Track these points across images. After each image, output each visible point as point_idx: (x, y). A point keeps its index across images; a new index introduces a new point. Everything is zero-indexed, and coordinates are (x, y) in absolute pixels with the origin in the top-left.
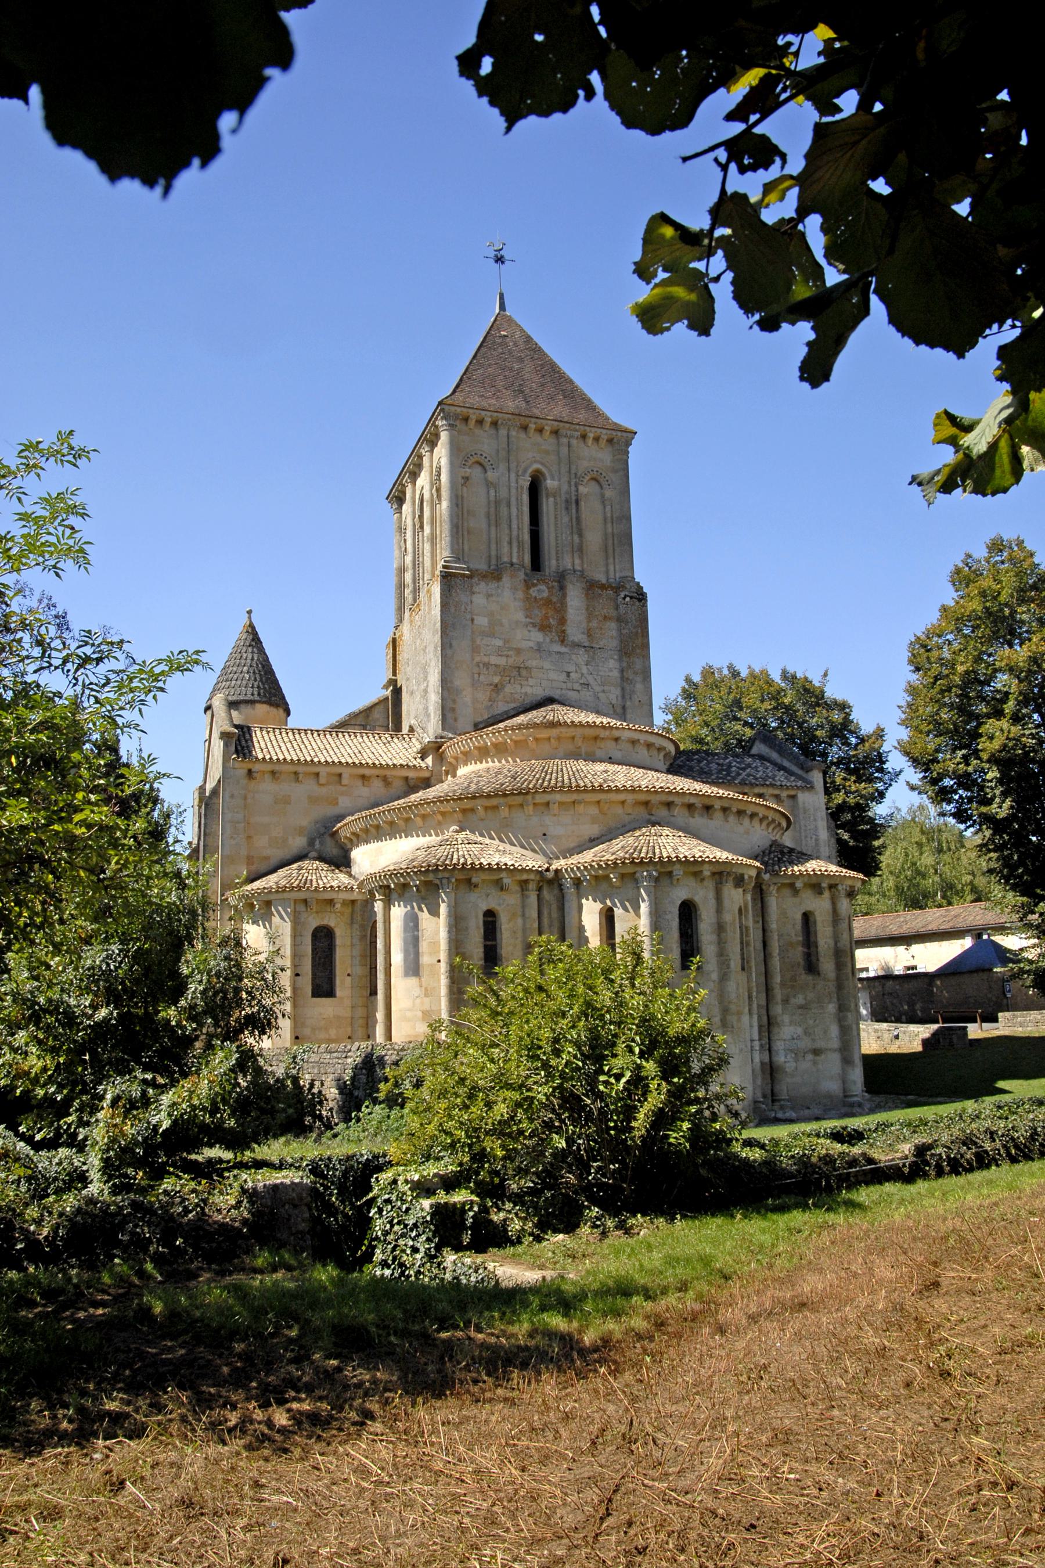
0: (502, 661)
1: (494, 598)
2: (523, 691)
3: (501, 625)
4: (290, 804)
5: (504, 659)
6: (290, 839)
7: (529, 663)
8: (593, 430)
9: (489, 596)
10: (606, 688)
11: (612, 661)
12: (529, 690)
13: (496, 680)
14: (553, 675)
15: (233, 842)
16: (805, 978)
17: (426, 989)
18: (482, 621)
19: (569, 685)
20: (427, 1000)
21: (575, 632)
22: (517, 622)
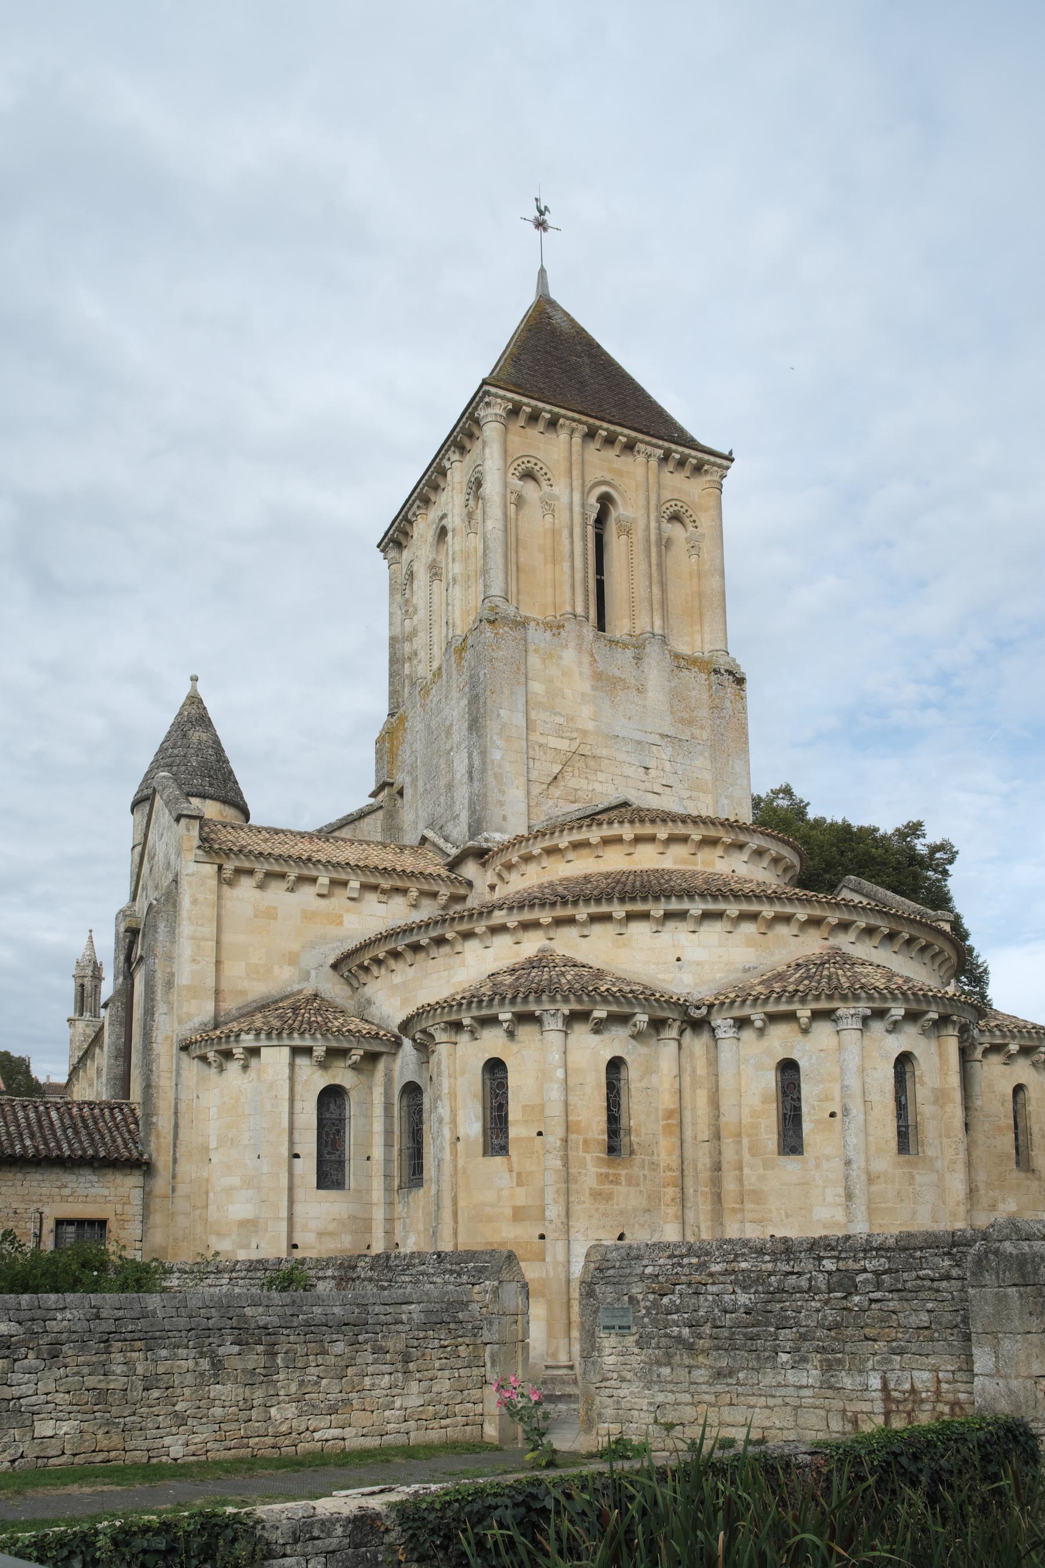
0: (563, 745)
2: (590, 788)
4: (275, 919)
5: (566, 742)
6: (276, 967)
7: (598, 752)
10: (694, 794)
12: (598, 787)
13: (556, 769)
14: (629, 771)
15: (196, 967)
16: (1015, 1176)
17: (519, 1175)
18: (537, 687)
19: (648, 786)
20: (521, 1191)
22: (583, 695)
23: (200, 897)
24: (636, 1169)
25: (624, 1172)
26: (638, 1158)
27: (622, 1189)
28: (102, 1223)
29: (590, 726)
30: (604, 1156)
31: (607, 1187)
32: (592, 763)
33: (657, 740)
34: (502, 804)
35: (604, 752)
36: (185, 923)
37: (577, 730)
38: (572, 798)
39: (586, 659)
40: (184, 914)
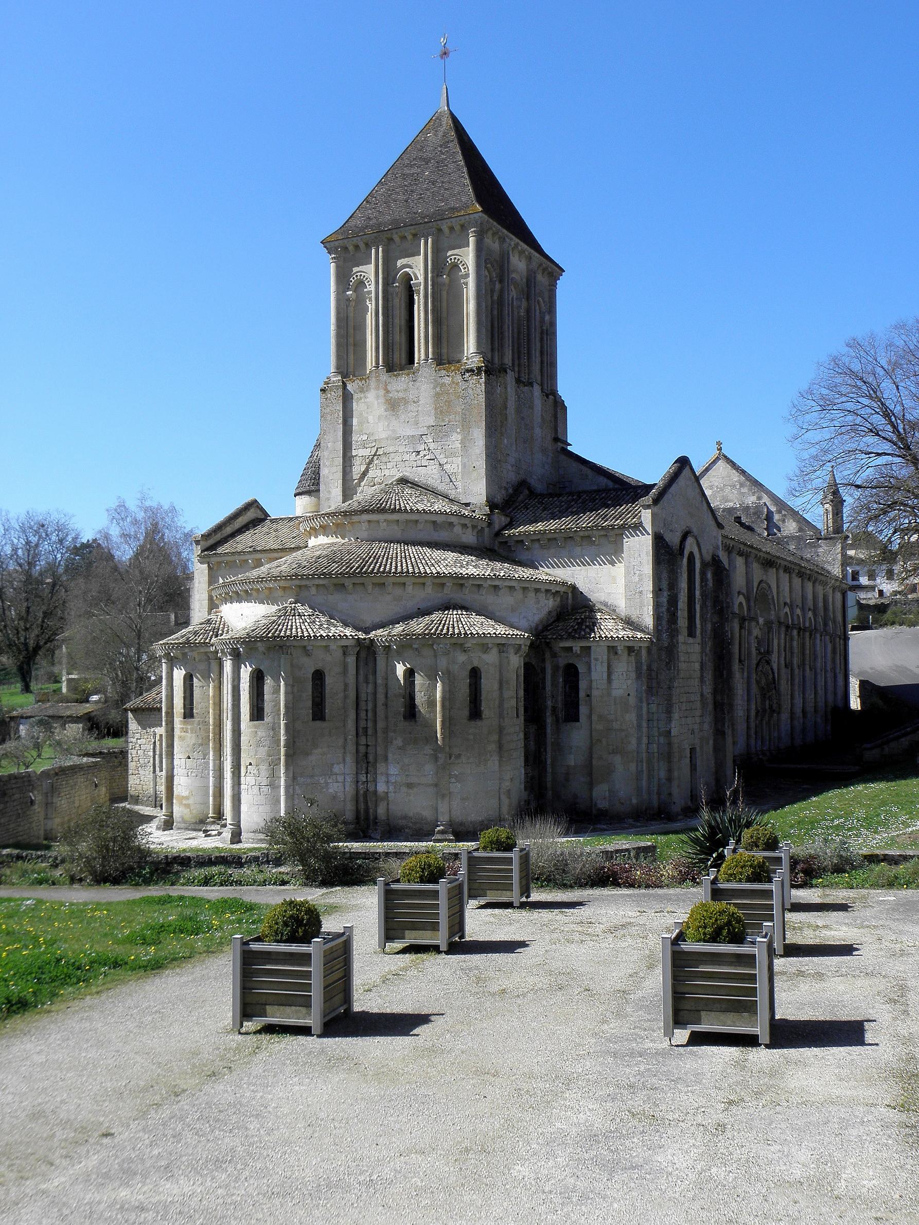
0: (367, 452)
1: (363, 401)
2: (383, 474)
10: (449, 460)
12: (387, 472)
13: (363, 468)
14: (406, 457)
19: (419, 463)
29: (383, 435)
32: (384, 459)
33: (424, 430)
34: (328, 499)
35: (391, 449)
36: (196, 593)
39: (382, 392)
40: (196, 589)
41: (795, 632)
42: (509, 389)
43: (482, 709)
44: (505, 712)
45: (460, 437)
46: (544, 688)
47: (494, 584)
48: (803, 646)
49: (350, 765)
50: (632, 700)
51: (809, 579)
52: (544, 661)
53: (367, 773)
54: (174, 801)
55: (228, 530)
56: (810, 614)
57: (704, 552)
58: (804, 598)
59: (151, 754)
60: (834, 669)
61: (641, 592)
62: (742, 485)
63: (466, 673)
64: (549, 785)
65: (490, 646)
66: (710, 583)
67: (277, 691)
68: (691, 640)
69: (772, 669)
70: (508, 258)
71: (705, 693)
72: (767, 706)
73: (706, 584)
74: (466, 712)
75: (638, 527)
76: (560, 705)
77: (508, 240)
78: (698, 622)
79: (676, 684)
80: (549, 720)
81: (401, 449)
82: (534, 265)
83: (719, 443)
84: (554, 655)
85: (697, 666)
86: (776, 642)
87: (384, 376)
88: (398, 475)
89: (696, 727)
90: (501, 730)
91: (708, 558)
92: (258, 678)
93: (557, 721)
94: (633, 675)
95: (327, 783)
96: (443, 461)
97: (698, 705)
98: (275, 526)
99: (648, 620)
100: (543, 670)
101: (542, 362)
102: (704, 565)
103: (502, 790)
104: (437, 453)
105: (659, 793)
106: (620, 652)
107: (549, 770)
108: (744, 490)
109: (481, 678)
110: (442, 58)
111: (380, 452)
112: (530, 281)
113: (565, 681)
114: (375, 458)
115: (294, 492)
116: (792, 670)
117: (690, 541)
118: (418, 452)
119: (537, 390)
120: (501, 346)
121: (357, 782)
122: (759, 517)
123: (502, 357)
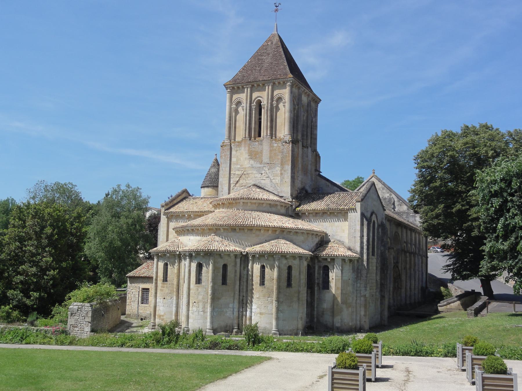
0: (240, 173)
1: (238, 151)
3: (240, 160)
8: (276, 80)
9: (236, 151)
10: (275, 178)
11: (278, 167)
12: (248, 182)
14: (257, 175)
19: (262, 178)
21: (266, 158)
22: (246, 158)
23: (164, 222)
24: (168, 285)
25: (165, 286)
26: (168, 283)
27: (165, 289)
28: (148, 289)
29: (248, 166)
30: (162, 282)
31: (162, 288)
32: (247, 176)
35: (250, 172)
36: (161, 228)
37: (243, 168)
38: (241, 186)
39: (247, 148)
40: (161, 226)
41: (408, 254)
42: (300, 149)
43: (292, 283)
44: (301, 284)
45: (280, 169)
46: (314, 275)
47: (296, 231)
48: (410, 260)
49: (236, 305)
50: (350, 282)
51: (414, 231)
52: (314, 264)
53: (243, 308)
54: (156, 317)
55: (175, 202)
56: (413, 247)
57: (379, 221)
58: (411, 239)
59: (137, 296)
60: (422, 270)
61: (355, 237)
62: (383, 189)
63: (286, 268)
64: (315, 316)
65: (296, 257)
66: (380, 234)
67: (208, 272)
68: (373, 257)
69: (399, 270)
70: (301, 96)
71: (377, 279)
72: (396, 286)
73: (379, 234)
74: (286, 284)
75: (354, 210)
76: (321, 282)
77: (301, 89)
78: (376, 249)
79: (368, 276)
80: (316, 289)
81: (254, 172)
82: (310, 99)
83: (374, 170)
84: (319, 261)
85: (375, 268)
86: (400, 258)
87: (248, 142)
88: (253, 183)
89: (374, 294)
90: (299, 292)
91: (380, 223)
92: (200, 267)
93: (319, 288)
94: (351, 271)
95: (226, 312)
96: (272, 178)
97: (375, 284)
98: (195, 201)
99: (358, 249)
100: (314, 268)
101: (311, 138)
102: (379, 226)
103: (299, 317)
104: (270, 175)
105: (360, 321)
106: (346, 261)
107: (316, 309)
108: (384, 191)
109: (292, 270)
110: (275, 12)
111: (245, 173)
112: (309, 104)
113: (323, 273)
114: (243, 175)
115: (201, 186)
116: (406, 271)
117: (374, 216)
118: (262, 174)
119: (310, 149)
120: (297, 131)
121: (239, 311)
122: (390, 203)
123: (297, 136)
